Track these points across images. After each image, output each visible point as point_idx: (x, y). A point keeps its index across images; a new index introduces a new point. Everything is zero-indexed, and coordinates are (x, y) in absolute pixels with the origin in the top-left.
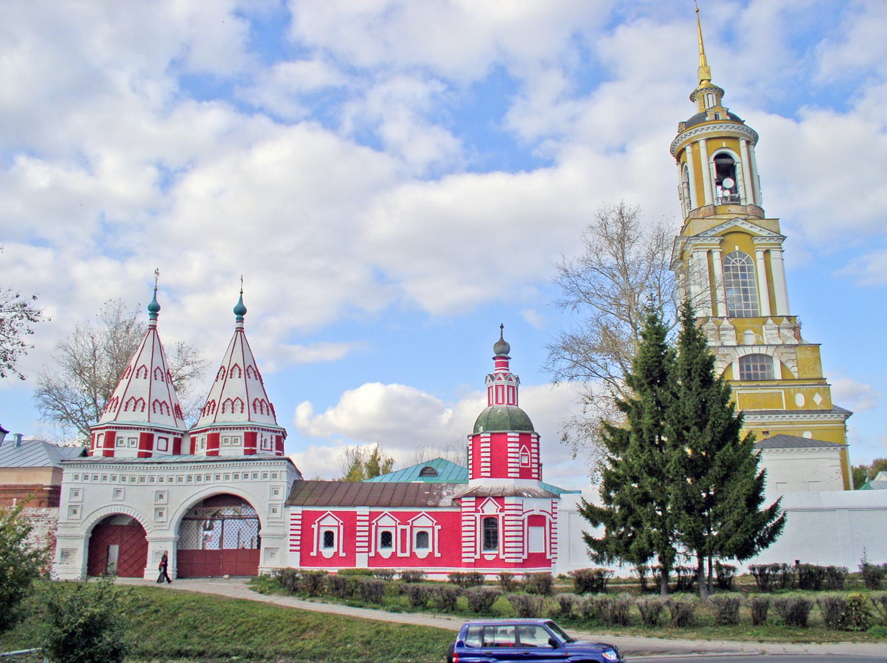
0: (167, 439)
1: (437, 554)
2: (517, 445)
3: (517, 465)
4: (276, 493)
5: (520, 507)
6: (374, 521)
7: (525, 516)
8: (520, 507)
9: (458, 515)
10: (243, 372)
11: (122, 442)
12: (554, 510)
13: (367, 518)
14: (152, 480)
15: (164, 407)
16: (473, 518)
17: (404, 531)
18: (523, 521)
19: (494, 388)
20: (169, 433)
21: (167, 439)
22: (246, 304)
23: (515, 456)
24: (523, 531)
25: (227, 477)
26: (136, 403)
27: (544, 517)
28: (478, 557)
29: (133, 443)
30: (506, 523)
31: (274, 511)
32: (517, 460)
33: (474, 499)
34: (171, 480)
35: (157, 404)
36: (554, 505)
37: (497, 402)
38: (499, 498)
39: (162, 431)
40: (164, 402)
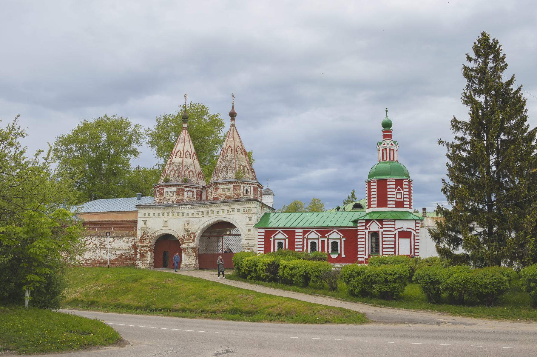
1: (343, 256)
2: (394, 186)
3: (394, 199)
4: (250, 220)
5: (393, 226)
6: (306, 236)
7: (397, 231)
8: (393, 226)
9: (356, 231)
11: (168, 194)
12: (417, 228)
13: (302, 234)
14: (183, 214)
15: (191, 173)
16: (364, 233)
17: (323, 242)
18: (395, 235)
19: (381, 150)
21: (192, 192)
22: (236, 110)
23: (393, 195)
24: (395, 241)
25: (223, 211)
27: (411, 232)
28: (366, 257)
30: (384, 236)
31: (249, 231)
32: (393, 196)
33: (364, 221)
34: (193, 214)
35: (187, 172)
36: (417, 225)
37: (383, 160)
38: (380, 221)
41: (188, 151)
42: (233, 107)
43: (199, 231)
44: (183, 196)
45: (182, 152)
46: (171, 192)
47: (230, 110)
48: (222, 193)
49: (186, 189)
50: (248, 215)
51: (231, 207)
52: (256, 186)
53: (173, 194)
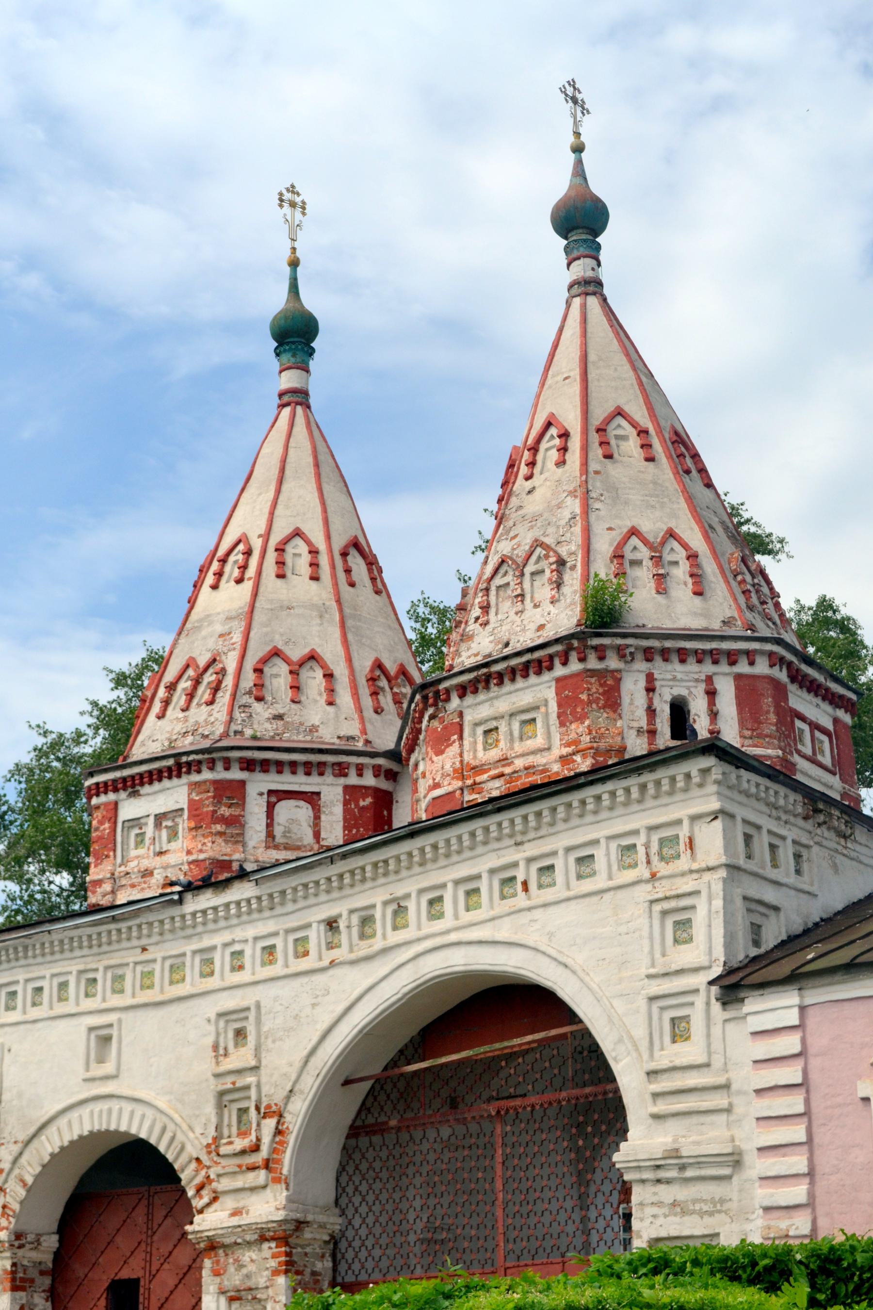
0: (312, 798)
4: (683, 930)
10: (575, 443)
20: (321, 769)
21: (312, 798)
22: (598, 187)
26: (197, 682)
29: (173, 834)
31: (679, 1030)
39: (280, 766)
40: (313, 657)
41: (298, 533)
42: (579, 171)
43: (310, 1084)
44: (239, 839)
45: (257, 544)
46: (160, 818)
47: (557, 186)
48: (483, 756)
49: (258, 785)
50: (663, 889)
51: (530, 850)
52: (762, 667)
53: (173, 834)
